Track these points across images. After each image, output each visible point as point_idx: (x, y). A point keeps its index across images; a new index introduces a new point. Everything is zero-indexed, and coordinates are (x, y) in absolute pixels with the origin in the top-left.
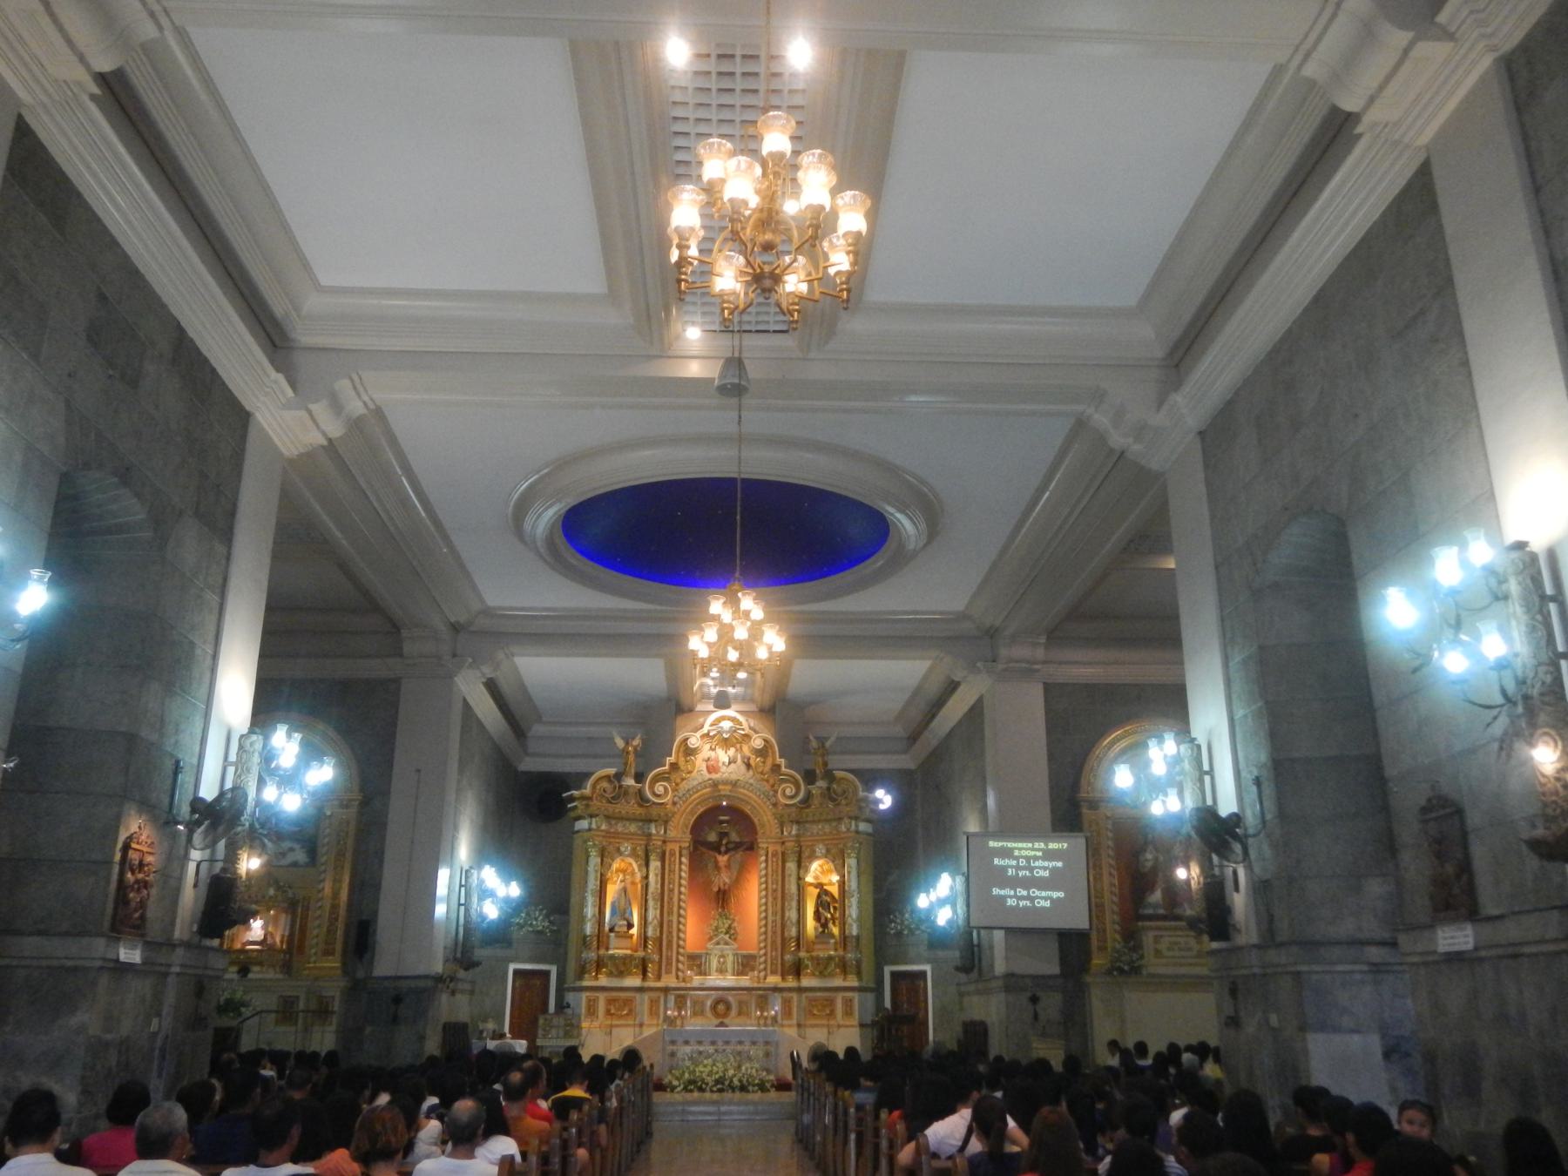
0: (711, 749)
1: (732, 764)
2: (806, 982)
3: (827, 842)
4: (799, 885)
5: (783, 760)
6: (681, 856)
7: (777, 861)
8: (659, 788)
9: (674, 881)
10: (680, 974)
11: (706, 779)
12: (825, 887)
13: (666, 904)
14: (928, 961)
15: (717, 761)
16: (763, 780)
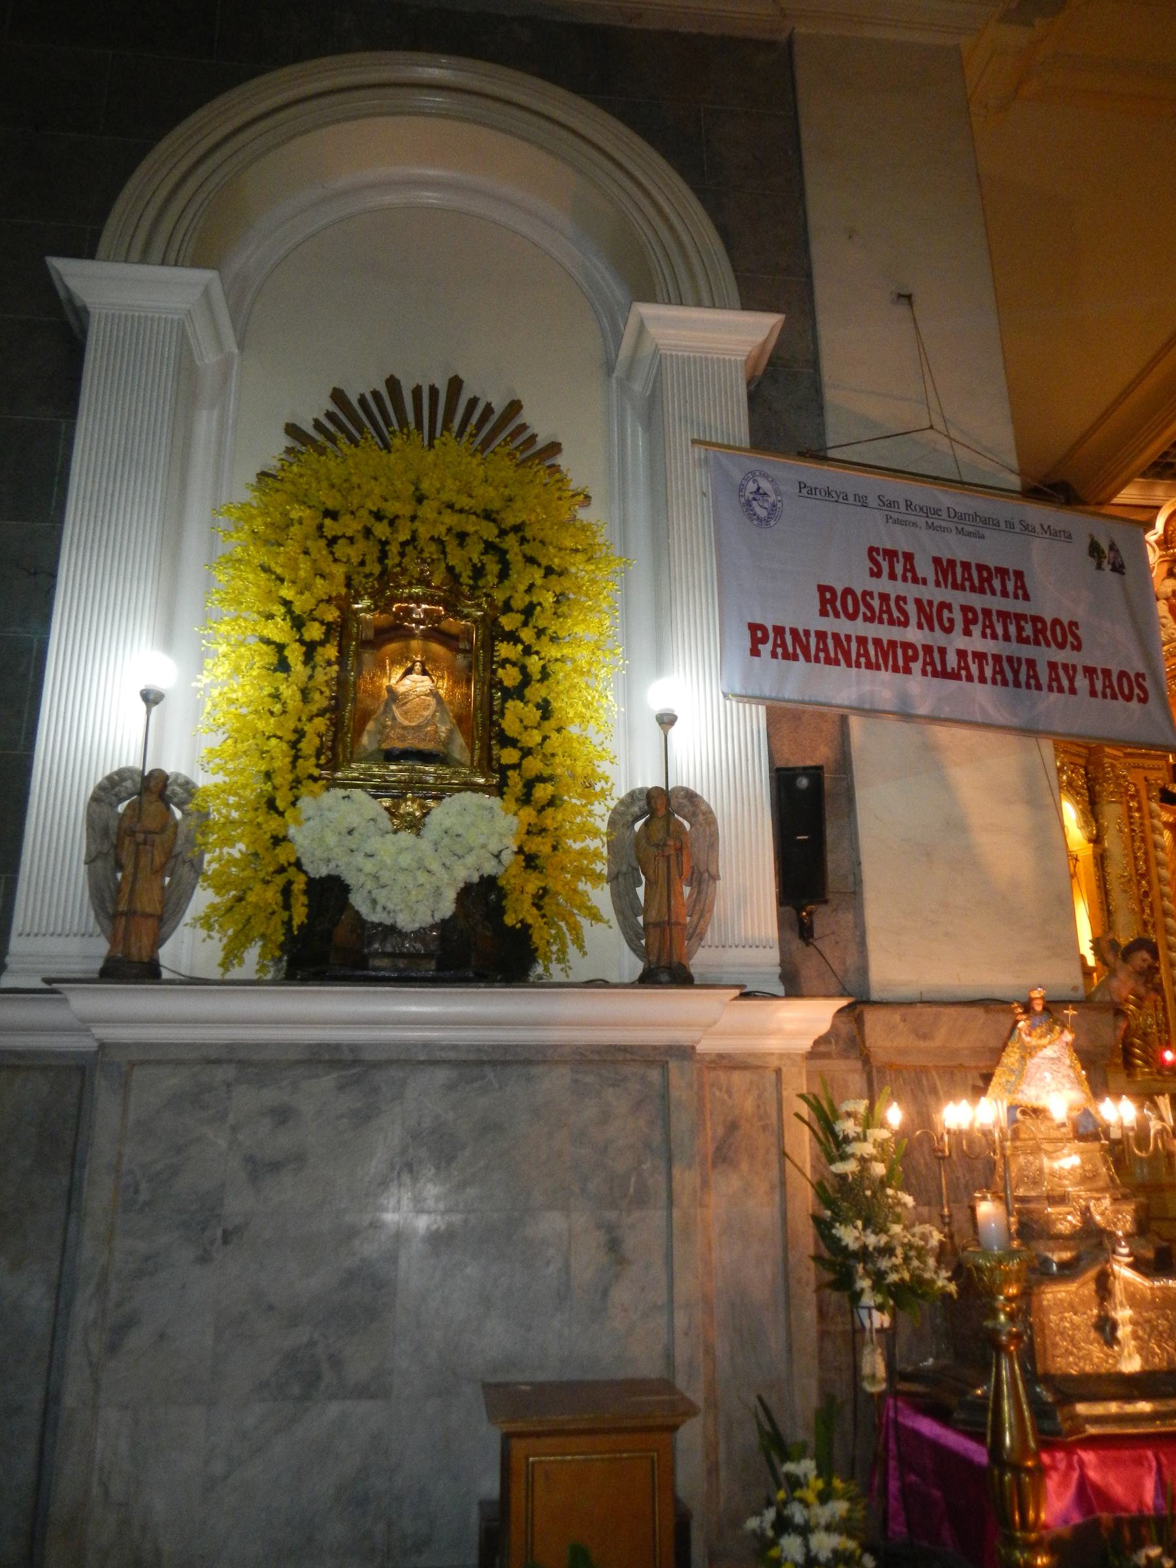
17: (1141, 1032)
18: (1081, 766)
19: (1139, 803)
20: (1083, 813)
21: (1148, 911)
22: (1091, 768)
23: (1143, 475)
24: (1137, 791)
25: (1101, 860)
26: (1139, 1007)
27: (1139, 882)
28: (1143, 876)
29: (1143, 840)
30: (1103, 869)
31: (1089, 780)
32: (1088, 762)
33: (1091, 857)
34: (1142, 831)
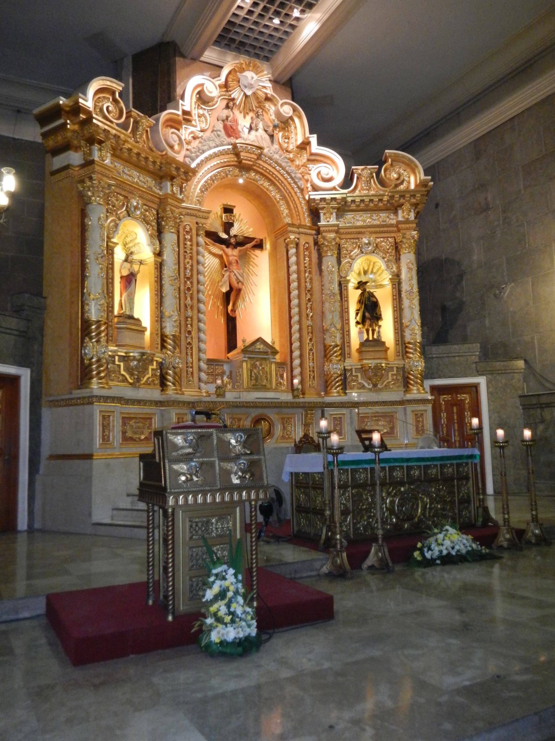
0: (227, 107)
1: (253, 132)
2: (354, 395)
3: (374, 235)
4: (340, 284)
5: (315, 136)
6: (198, 235)
7: (310, 257)
8: (174, 136)
9: (192, 266)
10: (202, 385)
11: (225, 143)
12: (367, 290)
13: (182, 295)
14: (480, 375)
15: (236, 121)
16: (289, 159)
17: (171, 366)
18: (154, 209)
19: (191, 236)
20: (151, 236)
21: (189, 299)
22: (160, 211)
23: (217, 42)
24: (191, 229)
25: (160, 267)
26: (173, 353)
27: (185, 282)
28: (188, 279)
29: (191, 258)
30: (161, 272)
31: (158, 218)
32: (159, 206)
33: (153, 264)
34: (191, 253)
